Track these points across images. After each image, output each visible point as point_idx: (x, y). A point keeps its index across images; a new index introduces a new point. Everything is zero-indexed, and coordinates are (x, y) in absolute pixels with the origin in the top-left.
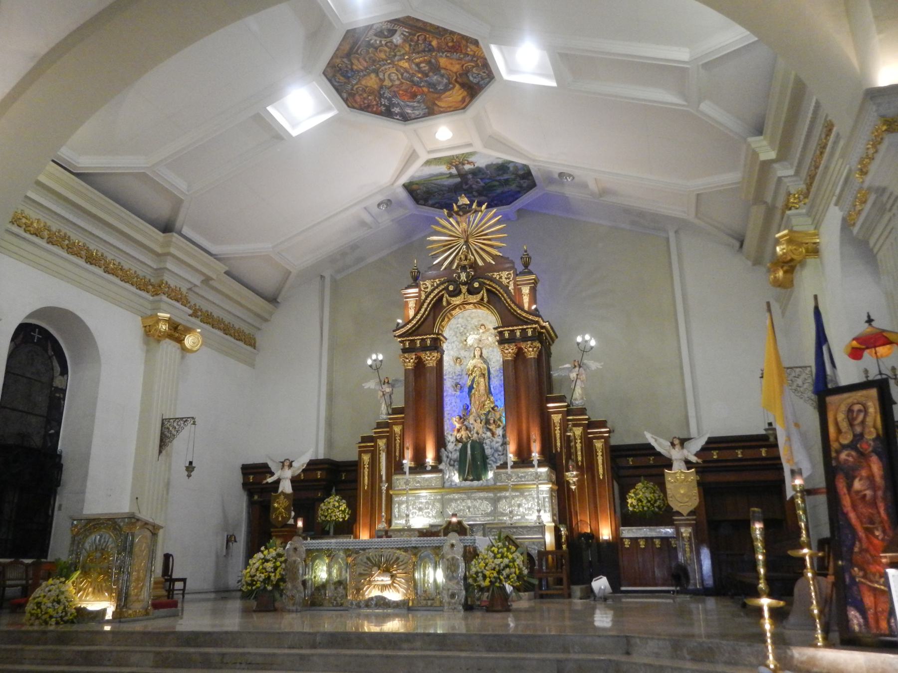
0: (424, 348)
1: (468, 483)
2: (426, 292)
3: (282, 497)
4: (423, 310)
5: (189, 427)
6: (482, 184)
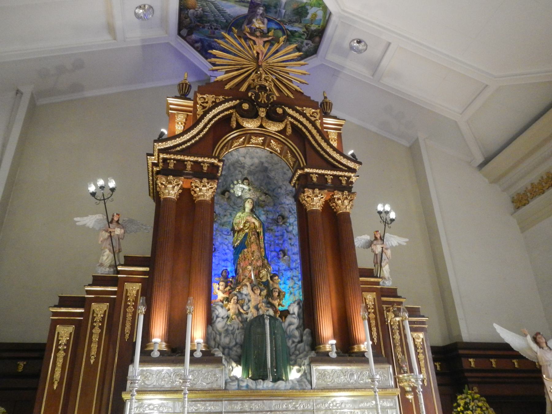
1: (268, 384)
2: (204, 107)
4: (201, 125)
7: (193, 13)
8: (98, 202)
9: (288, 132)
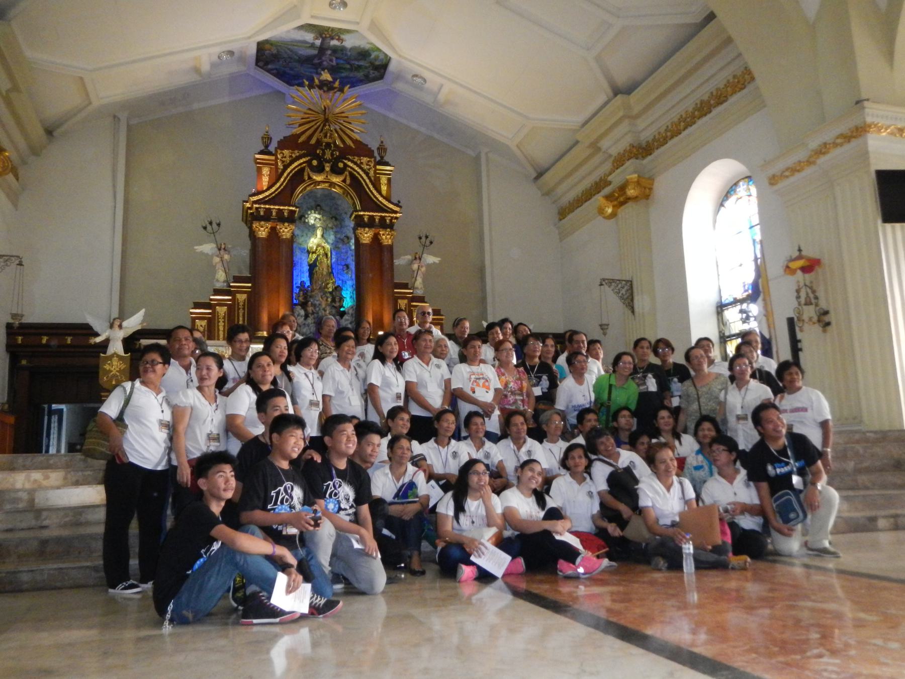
0: (281, 218)
3: (115, 358)
4: (282, 180)
5: (13, 265)
6: (334, 63)
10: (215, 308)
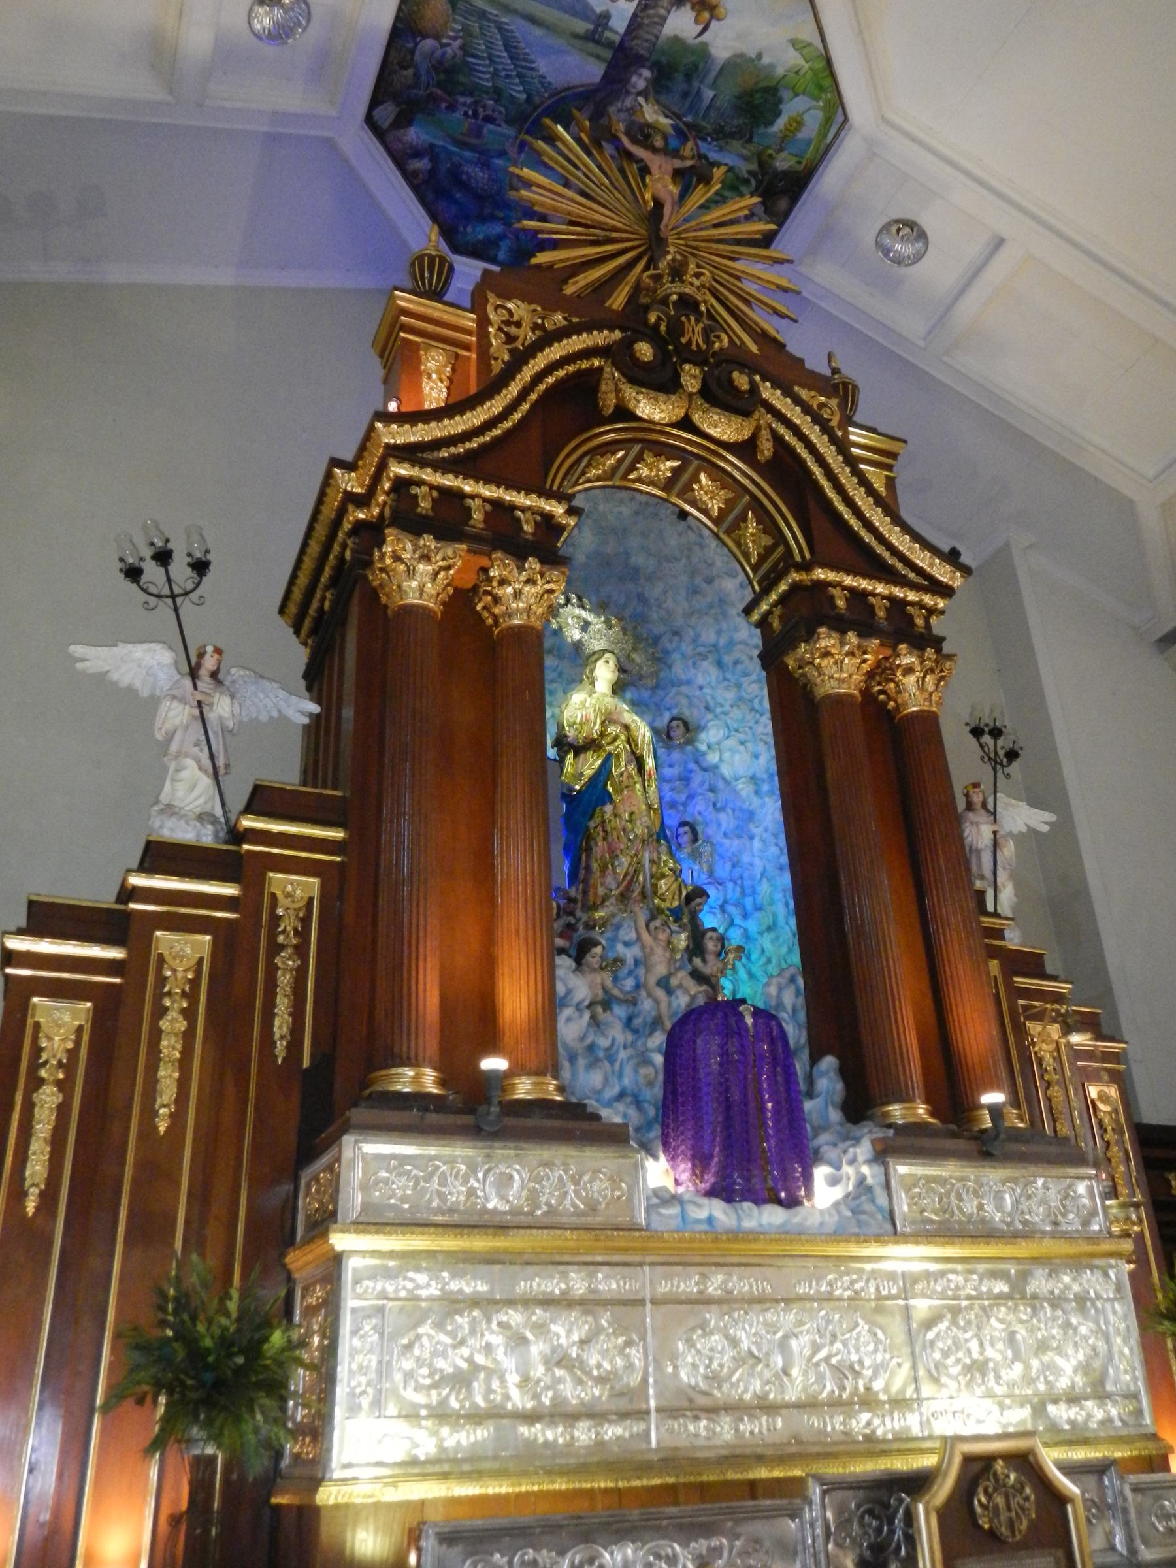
2: (510, 339)
4: (514, 389)
7: (433, 53)
8: (153, 601)
9: (762, 452)
10: (147, 941)
